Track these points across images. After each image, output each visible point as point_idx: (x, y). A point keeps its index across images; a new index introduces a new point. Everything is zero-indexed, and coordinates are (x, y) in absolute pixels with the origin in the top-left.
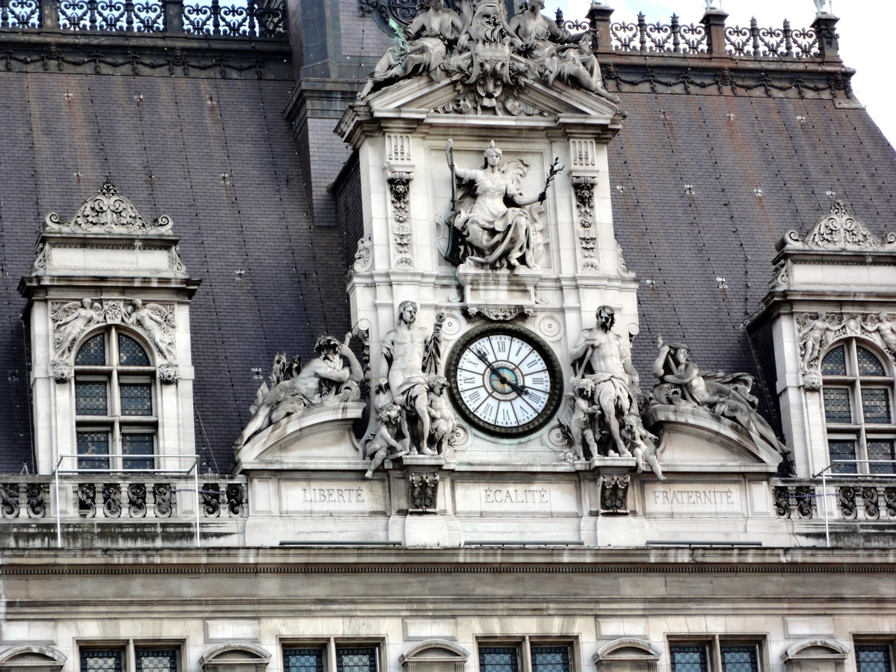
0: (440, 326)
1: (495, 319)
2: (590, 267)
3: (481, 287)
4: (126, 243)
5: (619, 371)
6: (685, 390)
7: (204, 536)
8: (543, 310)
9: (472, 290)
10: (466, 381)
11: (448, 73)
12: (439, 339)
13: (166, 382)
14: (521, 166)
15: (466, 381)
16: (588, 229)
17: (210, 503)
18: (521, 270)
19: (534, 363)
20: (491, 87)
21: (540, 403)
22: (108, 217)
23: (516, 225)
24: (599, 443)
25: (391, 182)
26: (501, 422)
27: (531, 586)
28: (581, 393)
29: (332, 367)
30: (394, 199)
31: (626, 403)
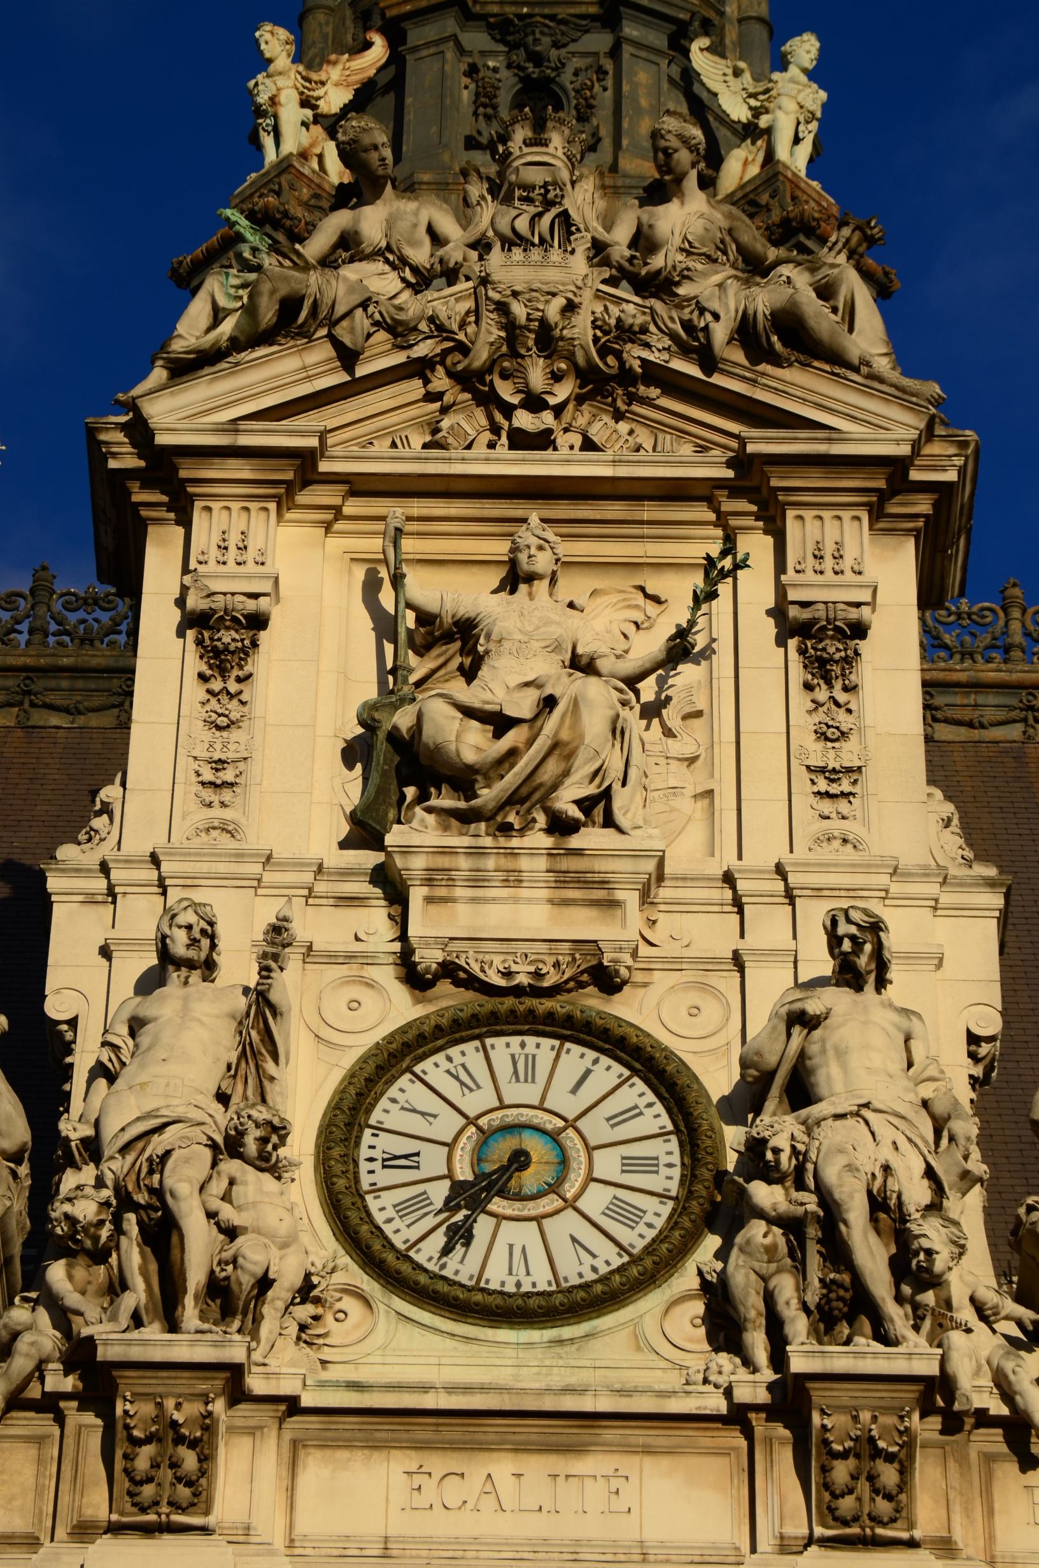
0: (275, 957)
1: (501, 982)
2: (836, 844)
3: (459, 892)
8: (674, 965)
9: (429, 900)
10: (390, 1162)
12: (274, 996)
14: (640, 599)
15: (390, 1162)
16: (836, 745)
19: (632, 1113)
20: (537, 375)
21: (641, 1228)
23: (575, 703)
30: (204, 668)
31: (917, 1194)
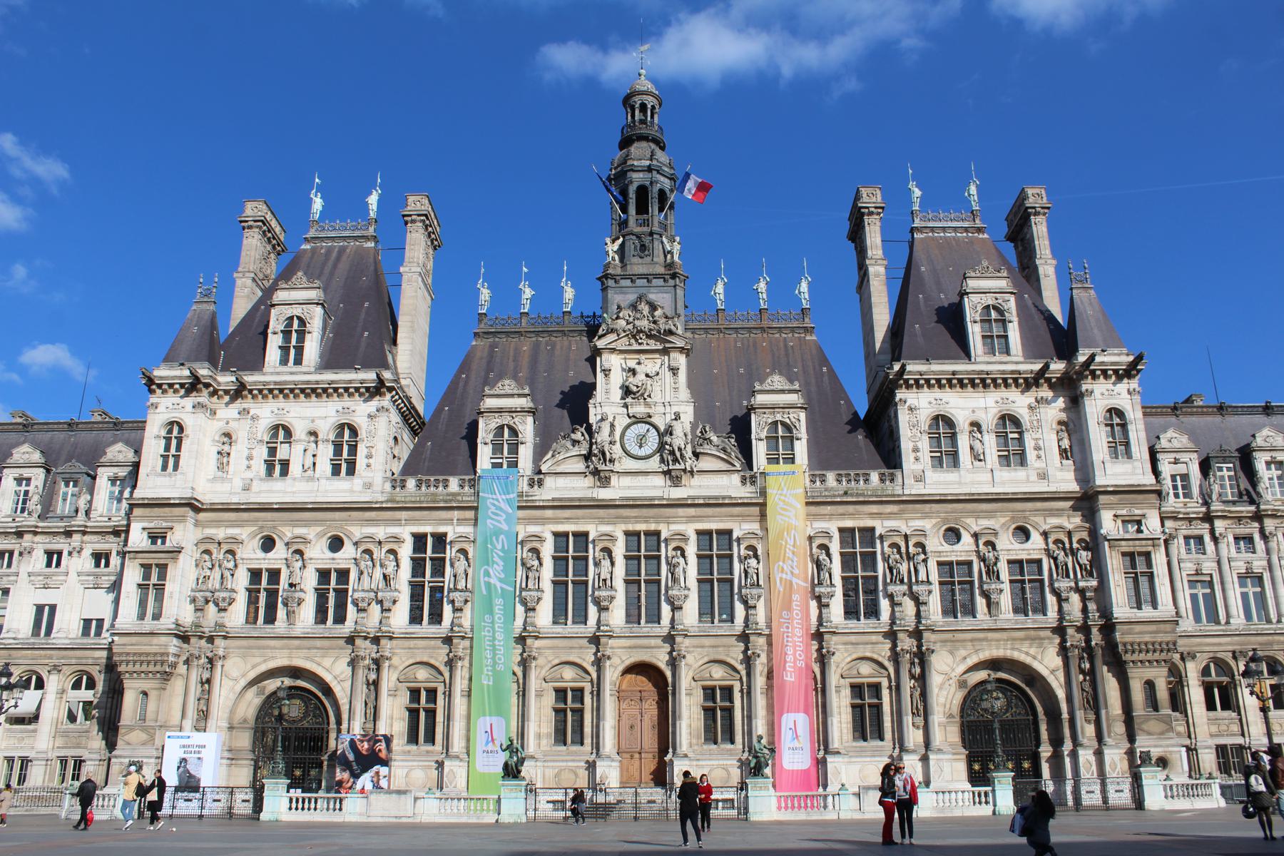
4: (512, 396)
5: (681, 435)
6: (711, 441)
7: (526, 496)
11: (624, 331)
13: (522, 443)
17: (531, 485)
18: (648, 400)
22: (507, 387)
24: (673, 461)
25: (604, 370)
26: (639, 454)
27: (645, 511)
28: (666, 443)
29: (578, 436)
31: (683, 447)
